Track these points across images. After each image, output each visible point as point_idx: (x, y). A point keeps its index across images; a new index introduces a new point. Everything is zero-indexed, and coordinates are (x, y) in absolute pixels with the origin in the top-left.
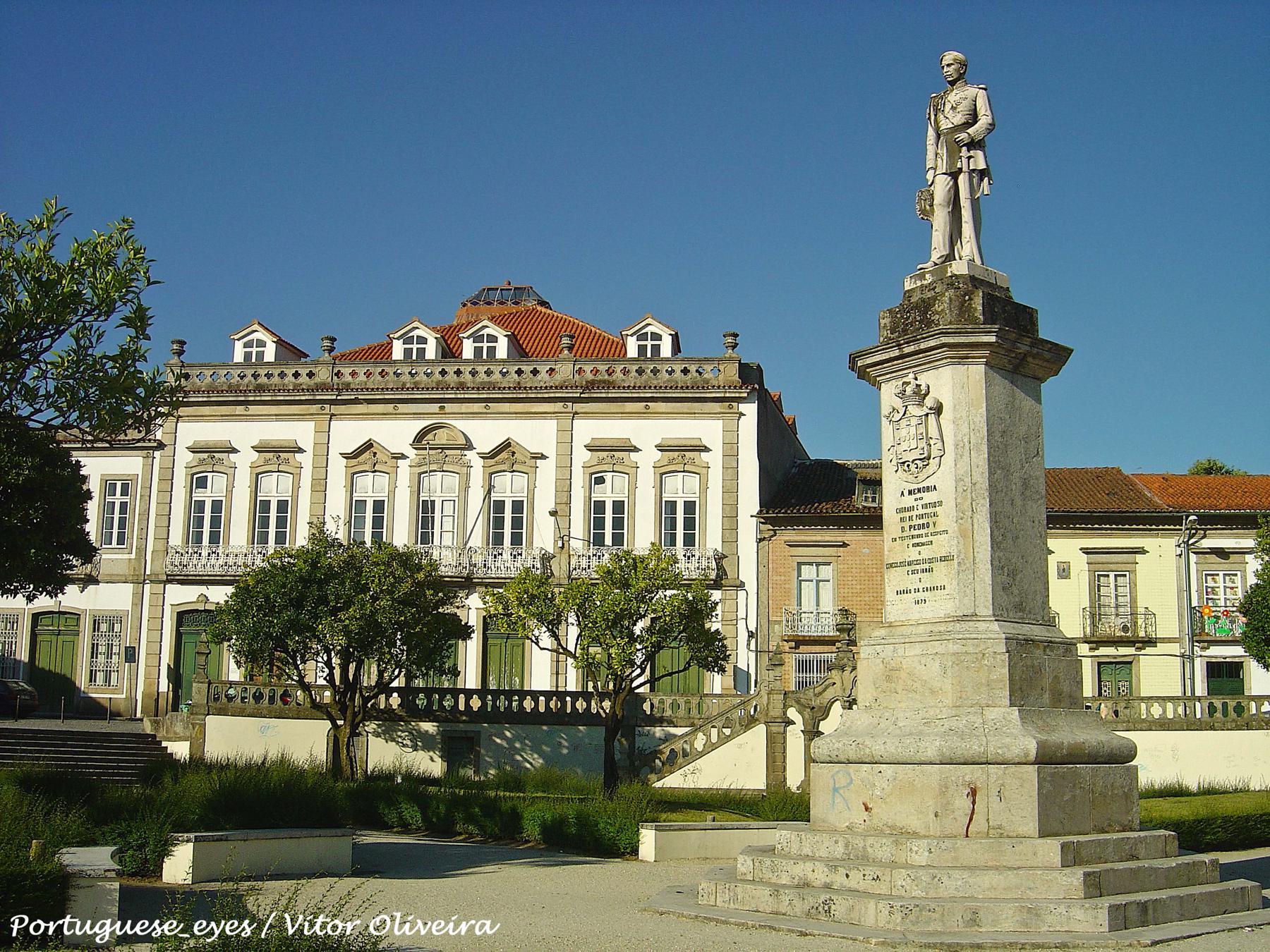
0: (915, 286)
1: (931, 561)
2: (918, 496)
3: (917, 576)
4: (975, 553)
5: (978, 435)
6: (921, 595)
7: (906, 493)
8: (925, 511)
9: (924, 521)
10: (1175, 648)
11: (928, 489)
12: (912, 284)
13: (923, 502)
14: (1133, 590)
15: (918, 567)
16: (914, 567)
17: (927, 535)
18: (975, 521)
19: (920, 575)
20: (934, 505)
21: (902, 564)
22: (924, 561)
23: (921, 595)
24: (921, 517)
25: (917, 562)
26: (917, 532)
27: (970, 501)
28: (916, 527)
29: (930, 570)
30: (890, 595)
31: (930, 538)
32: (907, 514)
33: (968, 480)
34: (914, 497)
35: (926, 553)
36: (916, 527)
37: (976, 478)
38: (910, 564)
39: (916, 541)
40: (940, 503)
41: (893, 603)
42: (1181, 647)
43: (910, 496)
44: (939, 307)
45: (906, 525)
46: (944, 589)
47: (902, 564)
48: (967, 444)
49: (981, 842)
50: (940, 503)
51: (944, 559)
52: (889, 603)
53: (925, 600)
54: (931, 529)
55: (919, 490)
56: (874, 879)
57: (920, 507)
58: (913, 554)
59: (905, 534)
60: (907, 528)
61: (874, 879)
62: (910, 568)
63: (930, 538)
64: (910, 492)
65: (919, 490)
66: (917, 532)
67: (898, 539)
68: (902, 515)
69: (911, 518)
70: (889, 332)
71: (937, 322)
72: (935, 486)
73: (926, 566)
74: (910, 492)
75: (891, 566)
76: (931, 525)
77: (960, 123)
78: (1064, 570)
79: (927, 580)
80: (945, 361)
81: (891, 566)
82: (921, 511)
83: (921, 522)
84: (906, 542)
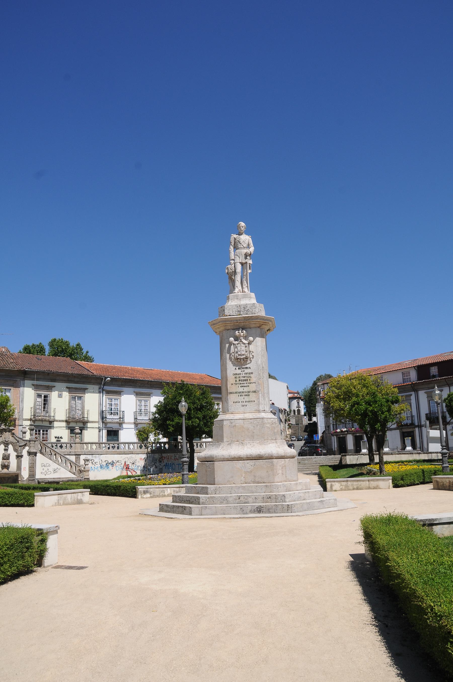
1: (249, 392)
2: (243, 370)
3: (243, 397)
6: (244, 404)
8: (245, 375)
9: (246, 379)
10: (96, 425)
13: (245, 372)
14: (84, 403)
16: (241, 394)
17: (247, 383)
19: (244, 397)
20: (250, 374)
21: (236, 393)
23: (244, 404)
26: (242, 382)
27: (262, 373)
28: (242, 381)
30: (230, 403)
31: (248, 385)
32: (238, 376)
33: (261, 366)
34: (241, 370)
35: (246, 389)
36: (242, 381)
37: (264, 365)
38: (240, 393)
39: (242, 385)
40: (252, 373)
42: (99, 425)
43: (239, 370)
45: (238, 380)
46: (254, 401)
47: (236, 393)
50: (252, 373)
51: (255, 392)
53: (246, 405)
55: (243, 368)
56: (268, 498)
58: (241, 390)
59: (236, 383)
60: (238, 380)
63: (248, 385)
66: (242, 382)
68: (236, 376)
69: (239, 377)
73: (247, 394)
74: (239, 369)
75: (231, 393)
76: (248, 380)
78: (60, 394)
79: (247, 398)
81: (231, 393)
82: (244, 375)
83: (244, 379)
84: (238, 385)
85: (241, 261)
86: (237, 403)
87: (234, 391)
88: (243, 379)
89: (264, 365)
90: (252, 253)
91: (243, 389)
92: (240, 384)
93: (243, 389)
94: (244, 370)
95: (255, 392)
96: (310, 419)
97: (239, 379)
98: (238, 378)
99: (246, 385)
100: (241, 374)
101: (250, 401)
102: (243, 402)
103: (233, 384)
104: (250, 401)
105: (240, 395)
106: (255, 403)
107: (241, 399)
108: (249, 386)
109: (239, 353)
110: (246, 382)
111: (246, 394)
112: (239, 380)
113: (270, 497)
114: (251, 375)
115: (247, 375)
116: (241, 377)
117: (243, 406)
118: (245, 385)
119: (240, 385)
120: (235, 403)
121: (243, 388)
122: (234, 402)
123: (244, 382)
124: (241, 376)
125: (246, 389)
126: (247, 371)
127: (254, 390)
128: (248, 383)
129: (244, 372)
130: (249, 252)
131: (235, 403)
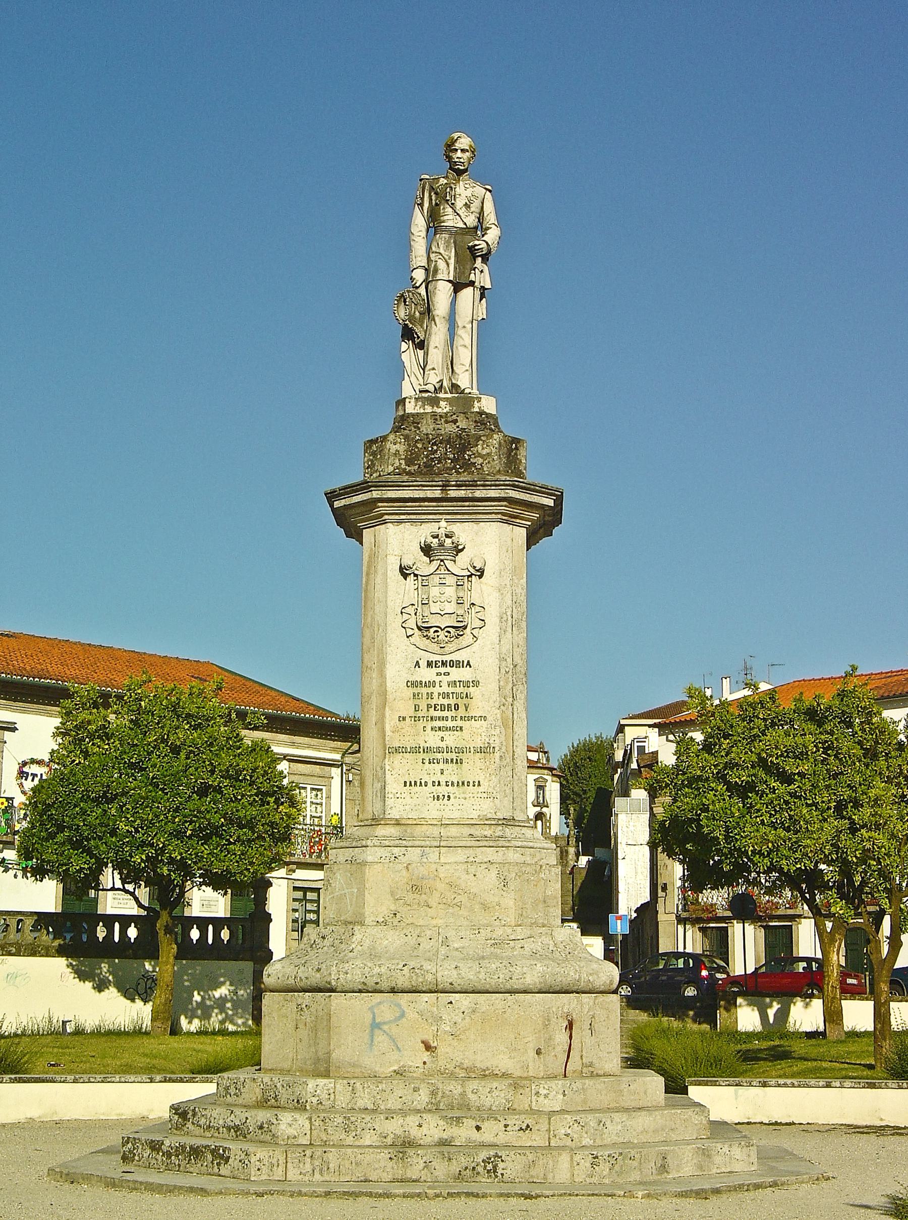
0: (422, 411)
1: (459, 750)
2: (443, 670)
3: (438, 767)
4: (515, 747)
5: (519, 609)
6: (443, 790)
7: (423, 664)
8: (451, 690)
9: (452, 702)
11: (452, 664)
12: (418, 407)
13: (448, 678)
15: (439, 756)
16: (431, 756)
17: (454, 718)
18: (515, 707)
19: (441, 766)
20: (466, 684)
21: (416, 750)
22: (449, 750)
23: (443, 790)
24: (446, 695)
25: (439, 750)
27: (511, 685)
29: (459, 762)
30: (393, 786)
31: (459, 723)
32: (424, 690)
33: (509, 660)
34: (435, 670)
35: (451, 739)
36: (439, 707)
37: (518, 659)
38: (427, 750)
40: (476, 683)
41: (398, 795)
44: (483, 449)
46: (479, 785)
47: (416, 750)
48: (510, 618)
49: (604, 1082)
50: (476, 683)
52: (390, 796)
53: (449, 796)
54: (462, 712)
55: (444, 664)
56: (521, 1129)
57: (444, 684)
58: (433, 739)
59: (420, 714)
60: (423, 705)
61: (521, 1129)
62: (427, 757)
63: (459, 723)
64: (429, 664)
65: (444, 664)
67: (408, 719)
68: (416, 690)
70: (403, 462)
71: (479, 467)
72: (468, 662)
73: (454, 756)
74: (429, 664)
77: (472, 226)
79: (452, 773)
80: (494, 516)
82: (445, 689)
83: (446, 702)
84: (421, 724)
85: (451, 278)
86: (418, 788)
87: (409, 743)
88: (442, 701)
89: (518, 659)
90: (493, 251)
91: (442, 739)
92: (432, 718)
93: (442, 739)
94: (448, 669)
95: (481, 751)
96: (830, 889)
97: (430, 701)
98: (425, 696)
99: (454, 724)
100: (437, 685)
101: (463, 783)
102: (439, 784)
103: (404, 719)
104: (463, 783)
105: (427, 762)
106: (481, 789)
107: (431, 773)
108: (461, 728)
109: (434, 608)
110: (453, 713)
111: (449, 756)
112: (429, 706)
113: (528, 1126)
114: (471, 690)
115: (458, 690)
116: (435, 695)
117: (438, 796)
118: (450, 724)
119: (430, 724)
120: (411, 785)
121: (441, 734)
122: (405, 782)
123: (445, 714)
124: (436, 690)
125: (451, 739)
126: (456, 674)
127: (479, 744)
128: (459, 718)
129: (448, 678)
130: (484, 245)
131: (411, 785)
